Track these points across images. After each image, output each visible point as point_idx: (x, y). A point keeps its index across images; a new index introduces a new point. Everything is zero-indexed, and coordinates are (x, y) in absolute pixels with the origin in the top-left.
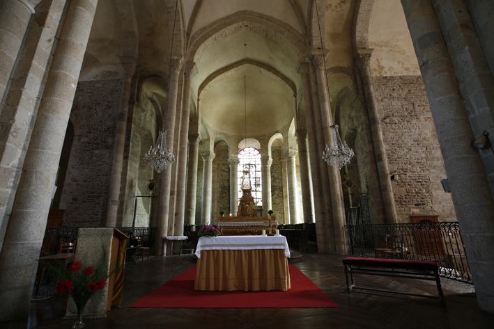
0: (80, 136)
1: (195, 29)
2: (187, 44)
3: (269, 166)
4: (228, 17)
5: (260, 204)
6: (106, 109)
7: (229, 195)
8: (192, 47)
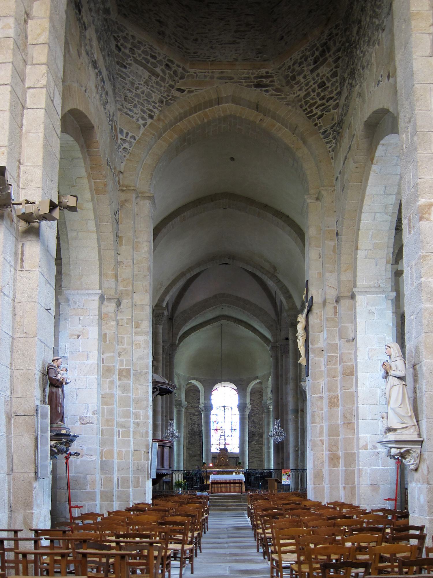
1: (176, 315)
5: (236, 450)
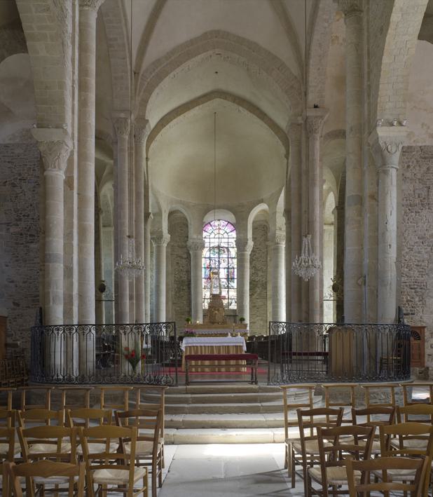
0: (8, 224)
1: (145, 65)
2: (136, 89)
3: (248, 252)
4: (192, 42)
5: (234, 306)
6: (34, 187)
7: (190, 293)
8: (142, 93)
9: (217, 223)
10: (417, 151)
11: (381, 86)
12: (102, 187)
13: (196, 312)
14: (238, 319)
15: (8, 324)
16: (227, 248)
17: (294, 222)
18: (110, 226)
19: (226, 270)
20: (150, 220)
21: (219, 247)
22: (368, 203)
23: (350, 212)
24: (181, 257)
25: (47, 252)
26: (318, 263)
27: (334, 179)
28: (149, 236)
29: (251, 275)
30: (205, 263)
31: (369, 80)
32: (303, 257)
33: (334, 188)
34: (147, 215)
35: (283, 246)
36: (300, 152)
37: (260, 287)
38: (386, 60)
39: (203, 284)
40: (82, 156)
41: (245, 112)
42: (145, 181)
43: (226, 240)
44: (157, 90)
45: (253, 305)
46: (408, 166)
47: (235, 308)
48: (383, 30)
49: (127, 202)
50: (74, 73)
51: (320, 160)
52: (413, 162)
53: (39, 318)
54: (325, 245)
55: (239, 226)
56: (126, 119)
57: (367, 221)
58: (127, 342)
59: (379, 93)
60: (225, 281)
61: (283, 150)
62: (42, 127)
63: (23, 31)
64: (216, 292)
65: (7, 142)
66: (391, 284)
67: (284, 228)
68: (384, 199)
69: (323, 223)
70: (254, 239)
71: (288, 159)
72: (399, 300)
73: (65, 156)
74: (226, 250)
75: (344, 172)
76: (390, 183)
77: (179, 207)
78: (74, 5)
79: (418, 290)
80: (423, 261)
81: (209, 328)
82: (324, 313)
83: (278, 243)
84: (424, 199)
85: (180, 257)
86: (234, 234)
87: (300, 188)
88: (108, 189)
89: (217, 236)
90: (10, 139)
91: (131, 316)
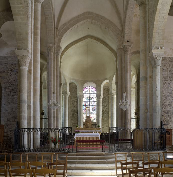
0: (5, 88)
1: (60, 26)
3: (101, 99)
4: (79, 16)
5: (95, 121)
6: (16, 73)
7: (78, 116)
8: (59, 36)
9: (89, 87)
10: (168, 59)
11: (154, 34)
12: (43, 73)
13: (80, 123)
14: (97, 126)
15: (5, 128)
16: (93, 98)
17: (119, 87)
18: (46, 89)
19: (92, 106)
20: (62, 86)
21: (89, 97)
22: (149, 79)
23: (142, 83)
24: (75, 101)
25: (20, 99)
26: (129, 103)
27: (135, 70)
28: (61, 93)
29: (102, 108)
30: (84, 103)
31: (149, 31)
32: (123, 101)
33: (136, 74)
34: (61, 84)
35: (115, 96)
36: (121, 60)
37: (106, 113)
38: (156, 23)
39: (83, 112)
40: (35, 61)
41: (100, 44)
42: (60, 71)
43: (92, 94)
44: (65, 35)
45: (103, 120)
46: (165, 65)
47: (96, 122)
48: (154, 11)
49: (53, 79)
50: (32, 28)
51: (130, 63)
52: (167, 63)
53: (17, 125)
54: (132, 96)
55: (98, 89)
56: (52, 47)
57: (148, 87)
58: (52, 135)
59: (153, 36)
60: (92, 111)
61: (115, 59)
62: (19, 50)
63: (12, 12)
64: (88, 115)
65: (5, 55)
66: (158, 112)
67: (115, 89)
68: (155, 78)
69: (131, 88)
70: (103, 94)
71: (117, 62)
72: (161, 118)
73: (28, 61)
74: (92, 98)
75: (139, 67)
76: (157, 72)
77: (74, 81)
78: (32, 2)
79: (169, 114)
80: (171, 103)
81: (85, 130)
82: (132, 124)
83: (113, 96)
84: (171, 78)
85: (74, 101)
86: (96, 92)
87: (122, 74)
88: (45, 74)
89: (89, 93)
90: (6, 54)
91: (54, 125)
